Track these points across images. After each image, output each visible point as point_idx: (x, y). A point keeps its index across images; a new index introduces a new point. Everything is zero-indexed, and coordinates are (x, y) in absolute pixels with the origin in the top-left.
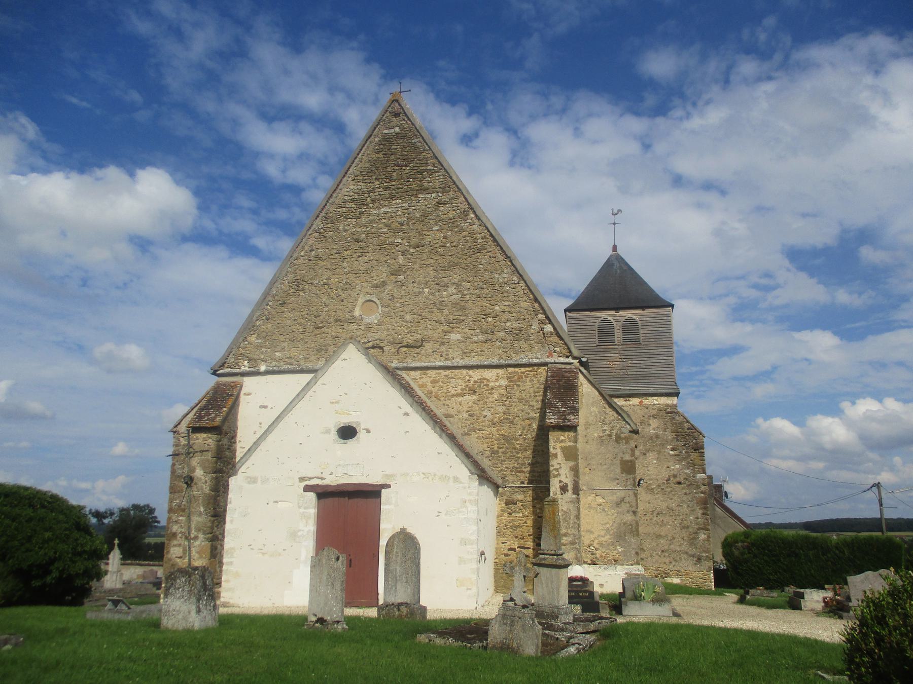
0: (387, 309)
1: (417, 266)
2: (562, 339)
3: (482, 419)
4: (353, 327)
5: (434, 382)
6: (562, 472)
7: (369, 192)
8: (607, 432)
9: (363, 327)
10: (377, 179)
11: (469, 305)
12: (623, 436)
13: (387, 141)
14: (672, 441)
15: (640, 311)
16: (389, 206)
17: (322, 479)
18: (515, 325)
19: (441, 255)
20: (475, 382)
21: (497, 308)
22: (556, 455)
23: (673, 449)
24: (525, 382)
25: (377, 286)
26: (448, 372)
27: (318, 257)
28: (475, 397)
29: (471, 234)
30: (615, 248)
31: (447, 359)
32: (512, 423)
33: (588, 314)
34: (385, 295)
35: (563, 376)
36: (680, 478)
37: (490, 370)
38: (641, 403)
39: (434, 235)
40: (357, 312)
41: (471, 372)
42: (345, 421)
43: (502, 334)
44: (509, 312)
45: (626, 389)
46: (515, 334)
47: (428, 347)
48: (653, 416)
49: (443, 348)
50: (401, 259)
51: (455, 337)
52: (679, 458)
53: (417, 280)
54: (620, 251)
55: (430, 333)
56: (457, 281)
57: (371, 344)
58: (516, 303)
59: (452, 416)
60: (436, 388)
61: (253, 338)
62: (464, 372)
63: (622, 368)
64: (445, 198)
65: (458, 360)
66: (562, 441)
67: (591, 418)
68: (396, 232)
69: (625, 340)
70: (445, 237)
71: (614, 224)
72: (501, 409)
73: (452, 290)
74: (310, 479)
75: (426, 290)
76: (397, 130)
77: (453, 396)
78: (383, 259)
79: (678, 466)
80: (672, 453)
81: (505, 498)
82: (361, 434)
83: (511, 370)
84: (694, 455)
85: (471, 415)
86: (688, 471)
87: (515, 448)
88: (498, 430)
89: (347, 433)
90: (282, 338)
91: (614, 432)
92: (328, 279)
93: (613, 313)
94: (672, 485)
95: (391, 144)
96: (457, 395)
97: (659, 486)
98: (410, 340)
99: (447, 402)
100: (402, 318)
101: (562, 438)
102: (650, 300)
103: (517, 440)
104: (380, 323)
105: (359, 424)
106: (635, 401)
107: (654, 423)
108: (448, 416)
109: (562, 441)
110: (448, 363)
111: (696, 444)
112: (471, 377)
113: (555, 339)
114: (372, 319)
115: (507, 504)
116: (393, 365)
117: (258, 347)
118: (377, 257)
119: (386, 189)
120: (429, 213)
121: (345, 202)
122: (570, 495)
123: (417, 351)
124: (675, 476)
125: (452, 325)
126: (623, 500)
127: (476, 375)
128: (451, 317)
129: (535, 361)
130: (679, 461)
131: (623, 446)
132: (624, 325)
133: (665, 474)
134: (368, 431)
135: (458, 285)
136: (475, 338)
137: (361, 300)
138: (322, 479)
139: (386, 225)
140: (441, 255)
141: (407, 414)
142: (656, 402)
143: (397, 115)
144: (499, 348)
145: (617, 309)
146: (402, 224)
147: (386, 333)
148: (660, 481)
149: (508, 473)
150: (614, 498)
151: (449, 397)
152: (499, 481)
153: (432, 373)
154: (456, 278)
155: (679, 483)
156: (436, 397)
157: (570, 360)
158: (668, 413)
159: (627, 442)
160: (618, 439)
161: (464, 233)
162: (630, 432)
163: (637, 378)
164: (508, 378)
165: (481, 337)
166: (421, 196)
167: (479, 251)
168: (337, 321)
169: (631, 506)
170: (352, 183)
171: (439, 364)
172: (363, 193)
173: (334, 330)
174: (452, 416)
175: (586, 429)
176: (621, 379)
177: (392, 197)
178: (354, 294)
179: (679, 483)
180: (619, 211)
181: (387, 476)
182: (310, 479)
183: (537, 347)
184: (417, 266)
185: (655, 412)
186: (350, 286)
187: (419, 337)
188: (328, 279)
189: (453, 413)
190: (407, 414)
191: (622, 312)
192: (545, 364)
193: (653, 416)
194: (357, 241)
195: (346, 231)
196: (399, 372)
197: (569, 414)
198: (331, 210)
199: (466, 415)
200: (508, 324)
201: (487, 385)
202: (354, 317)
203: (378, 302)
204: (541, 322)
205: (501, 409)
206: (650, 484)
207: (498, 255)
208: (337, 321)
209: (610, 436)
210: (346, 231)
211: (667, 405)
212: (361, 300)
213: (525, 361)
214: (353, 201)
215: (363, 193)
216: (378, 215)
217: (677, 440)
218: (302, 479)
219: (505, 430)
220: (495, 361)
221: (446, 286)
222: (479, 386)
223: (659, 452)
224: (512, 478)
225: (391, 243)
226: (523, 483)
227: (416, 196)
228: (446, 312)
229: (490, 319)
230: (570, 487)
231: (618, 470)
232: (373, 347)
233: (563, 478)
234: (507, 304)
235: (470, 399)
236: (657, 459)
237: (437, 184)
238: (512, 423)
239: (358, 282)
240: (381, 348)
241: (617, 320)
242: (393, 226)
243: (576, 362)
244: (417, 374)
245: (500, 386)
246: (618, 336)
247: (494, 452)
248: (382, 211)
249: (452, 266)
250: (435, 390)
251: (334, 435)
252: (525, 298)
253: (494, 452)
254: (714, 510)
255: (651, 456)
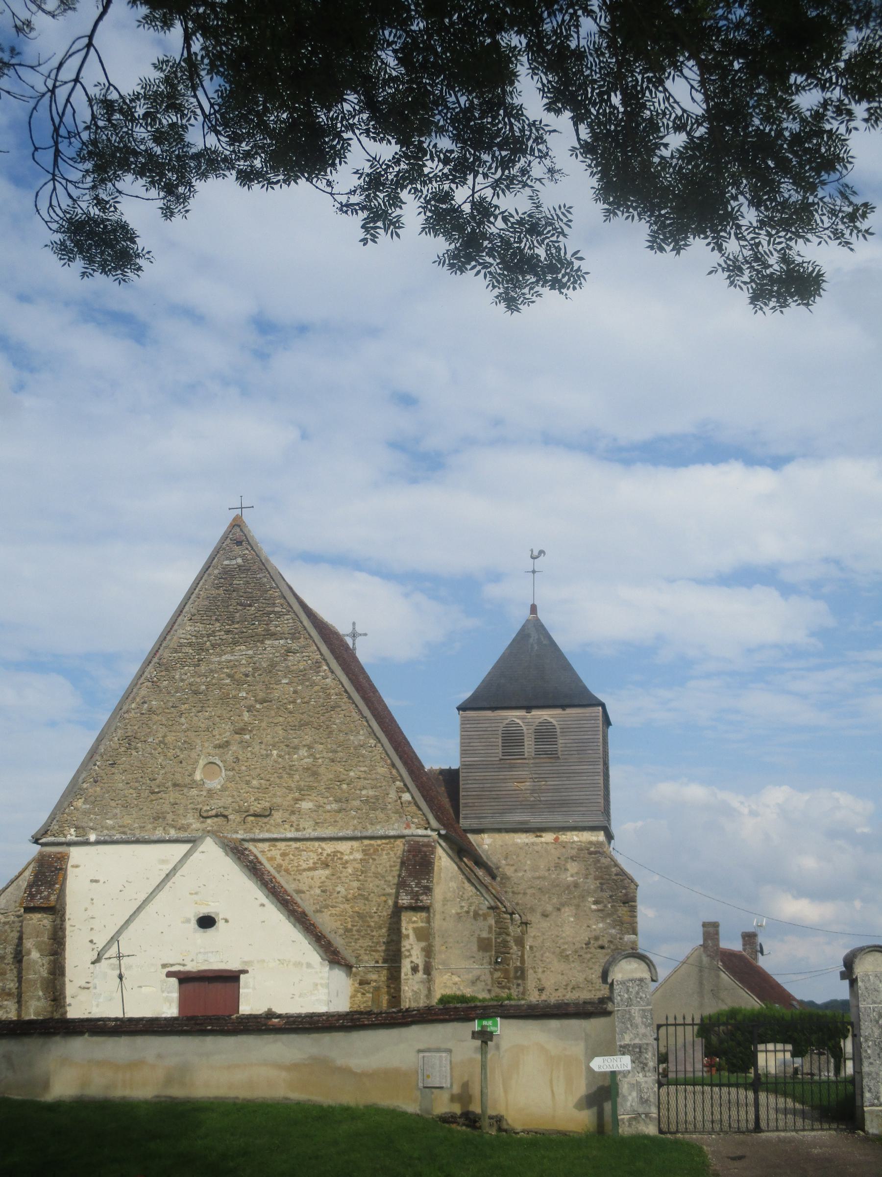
0: (231, 773)
1: (264, 724)
2: (420, 809)
3: (335, 895)
4: (194, 792)
5: (284, 855)
6: (414, 952)
7: (209, 636)
8: (465, 909)
9: (204, 793)
10: (217, 620)
11: (322, 770)
12: (481, 912)
13: (228, 574)
14: (595, 891)
15: (559, 711)
16: (232, 652)
17: (184, 965)
18: (371, 793)
19: (290, 713)
20: (328, 855)
21: (352, 774)
22: (408, 936)
23: (596, 903)
24: (381, 855)
25: (219, 746)
26: (298, 844)
27: (150, 711)
28: (327, 872)
29: (324, 689)
30: (534, 609)
31: (297, 830)
32: (367, 899)
33: (489, 713)
34: (229, 757)
35: (420, 851)
36: (604, 941)
37: (344, 843)
38: (556, 839)
39: (284, 688)
40: (198, 776)
41: (323, 844)
42: (204, 911)
43: (356, 803)
44: (365, 779)
45: (535, 820)
46: (373, 804)
47: (278, 816)
48: (572, 858)
49: (294, 818)
50: (246, 716)
51: (306, 805)
52: (603, 914)
53: (265, 740)
54: (542, 615)
55: (278, 800)
56: (308, 742)
57: (213, 813)
58: (372, 768)
59: (303, 892)
60: (287, 862)
61: (79, 803)
62: (316, 844)
63: (533, 791)
64: (295, 646)
65: (310, 831)
66: (414, 922)
67: (449, 894)
68: (239, 683)
69: (538, 753)
70: (295, 692)
71: (534, 572)
72: (356, 884)
73: (303, 752)
74: (172, 965)
75: (275, 752)
76: (239, 561)
77: (305, 870)
78: (225, 714)
79: (601, 925)
80: (594, 907)
81: (358, 978)
82: (220, 924)
83: (366, 842)
84: (623, 911)
85: (323, 891)
86: (613, 931)
87: (369, 926)
88: (352, 907)
89: (206, 922)
90: (113, 804)
91: (472, 908)
92: (164, 737)
93: (522, 713)
94: (593, 950)
95: (233, 577)
96: (310, 869)
97: (576, 952)
98: (257, 807)
99: (299, 877)
100: (248, 783)
101: (414, 919)
102: (575, 696)
103: (372, 917)
104: (224, 789)
105: (218, 914)
106: (548, 837)
107: (573, 867)
108: (299, 892)
109: (414, 922)
110: (299, 835)
111: (626, 895)
112: (323, 849)
113: (414, 808)
114: (215, 784)
115: (361, 983)
116: (239, 836)
117: (86, 813)
118: (219, 712)
119: (228, 632)
120: (277, 663)
121: (181, 645)
122: (420, 975)
123: (266, 820)
124: (597, 938)
125: (303, 792)
126: (478, 978)
127: (329, 848)
128: (302, 783)
129: (392, 833)
130: (603, 919)
131: (481, 923)
132: (537, 731)
133: (585, 936)
134: (227, 921)
135: (310, 747)
136: (328, 807)
137: (202, 762)
138: (184, 965)
139: (229, 676)
140: (290, 713)
141: (263, 905)
142: (576, 839)
143: (239, 543)
144: (354, 818)
145: (529, 708)
146: (247, 675)
147: (230, 800)
148: (578, 946)
149: (362, 952)
150: (470, 976)
151: (300, 871)
152: (353, 961)
153: (282, 845)
154: (308, 739)
155: (602, 947)
156: (287, 871)
157: (429, 832)
158: (591, 853)
159: (485, 919)
160: (476, 915)
161: (317, 688)
162: (488, 908)
163: (553, 806)
164: (363, 851)
165: (335, 806)
166: (267, 642)
167: (333, 708)
168: (175, 785)
169: (486, 984)
170: (189, 623)
171: (289, 835)
172: (202, 636)
173: (172, 795)
174: (303, 892)
175: (444, 905)
176: (532, 807)
177: (235, 643)
178: (194, 755)
179: (602, 947)
180: (542, 552)
181: (245, 963)
182: (172, 965)
183: (394, 817)
184: (264, 724)
185: (574, 852)
186: (189, 746)
187: (267, 805)
188: (164, 737)
189: (305, 889)
190: (263, 905)
191: (535, 712)
192: (403, 837)
193: (572, 858)
194: (196, 693)
195: (182, 680)
196: (246, 845)
197: (422, 894)
198: (166, 655)
199: (318, 891)
200: (364, 792)
201: (341, 859)
202: (194, 781)
203: (221, 764)
204: (399, 790)
205: (356, 884)
206: (564, 950)
207: (354, 714)
208: (175, 785)
209: (468, 912)
210: (182, 680)
211: (591, 843)
212: (202, 762)
213: (381, 833)
214: (190, 645)
215: (202, 636)
216: (219, 663)
217: (602, 890)
218: (164, 966)
219: (360, 906)
220: (349, 833)
221: (296, 748)
222: (333, 860)
223: (578, 906)
224: (366, 958)
225: (235, 697)
226: (377, 962)
227: (262, 642)
228: (297, 777)
229: (344, 786)
230: (421, 968)
231: (475, 948)
232: (216, 816)
233: (414, 959)
234: (362, 769)
235: (322, 873)
236: (576, 916)
237: (286, 630)
238: (367, 899)
239: (199, 742)
240: (226, 817)
241: (528, 724)
242: (236, 677)
243: (434, 834)
244: (265, 846)
245: (355, 860)
246: (529, 746)
247: (347, 930)
248: (224, 658)
249: (303, 725)
250: (285, 864)
251: (193, 924)
252: (382, 763)
253: (347, 930)
254: (718, 976)
255: (568, 913)
